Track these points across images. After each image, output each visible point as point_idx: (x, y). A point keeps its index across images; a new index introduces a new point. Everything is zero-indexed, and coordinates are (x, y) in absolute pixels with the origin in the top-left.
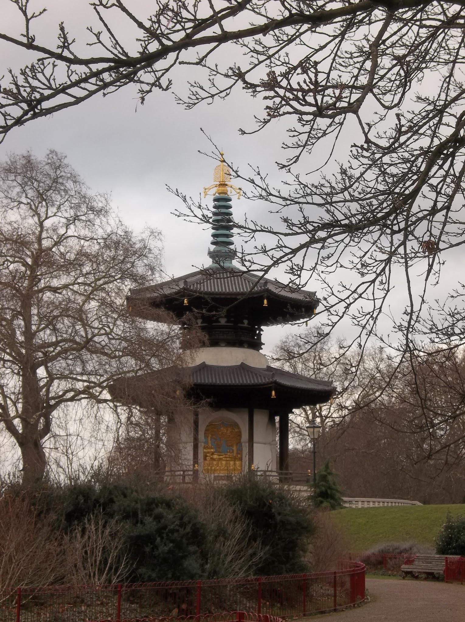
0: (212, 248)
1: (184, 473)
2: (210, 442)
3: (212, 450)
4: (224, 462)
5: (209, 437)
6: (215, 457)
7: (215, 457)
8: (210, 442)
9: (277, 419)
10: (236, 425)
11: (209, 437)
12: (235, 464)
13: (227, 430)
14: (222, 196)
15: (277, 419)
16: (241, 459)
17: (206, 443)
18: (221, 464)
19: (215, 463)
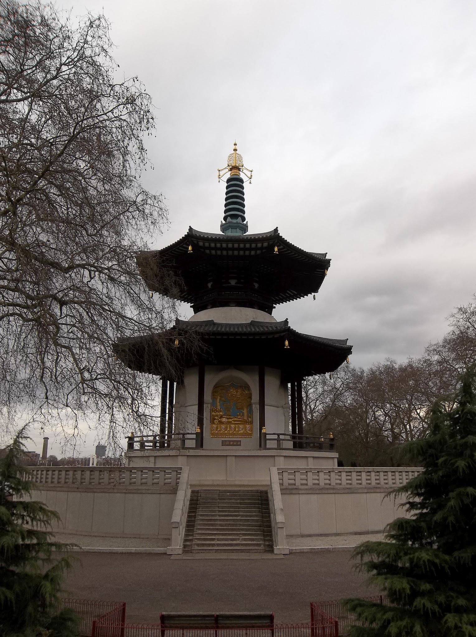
0: (224, 222)
1: (184, 437)
2: (218, 404)
3: (221, 413)
4: (233, 426)
5: (218, 400)
6: (224, 420)
7: (224, 420)
8: (218, 404)
9: (289, 385)
10: (247, 387)
11: (218, 400)
12: (245, 428)
13: (237, 392)
14: (235, 177)
15: (289, 385)
16: (251, 423)
17: (213, 404)
18: (230, 427)
19: (223, 426)
